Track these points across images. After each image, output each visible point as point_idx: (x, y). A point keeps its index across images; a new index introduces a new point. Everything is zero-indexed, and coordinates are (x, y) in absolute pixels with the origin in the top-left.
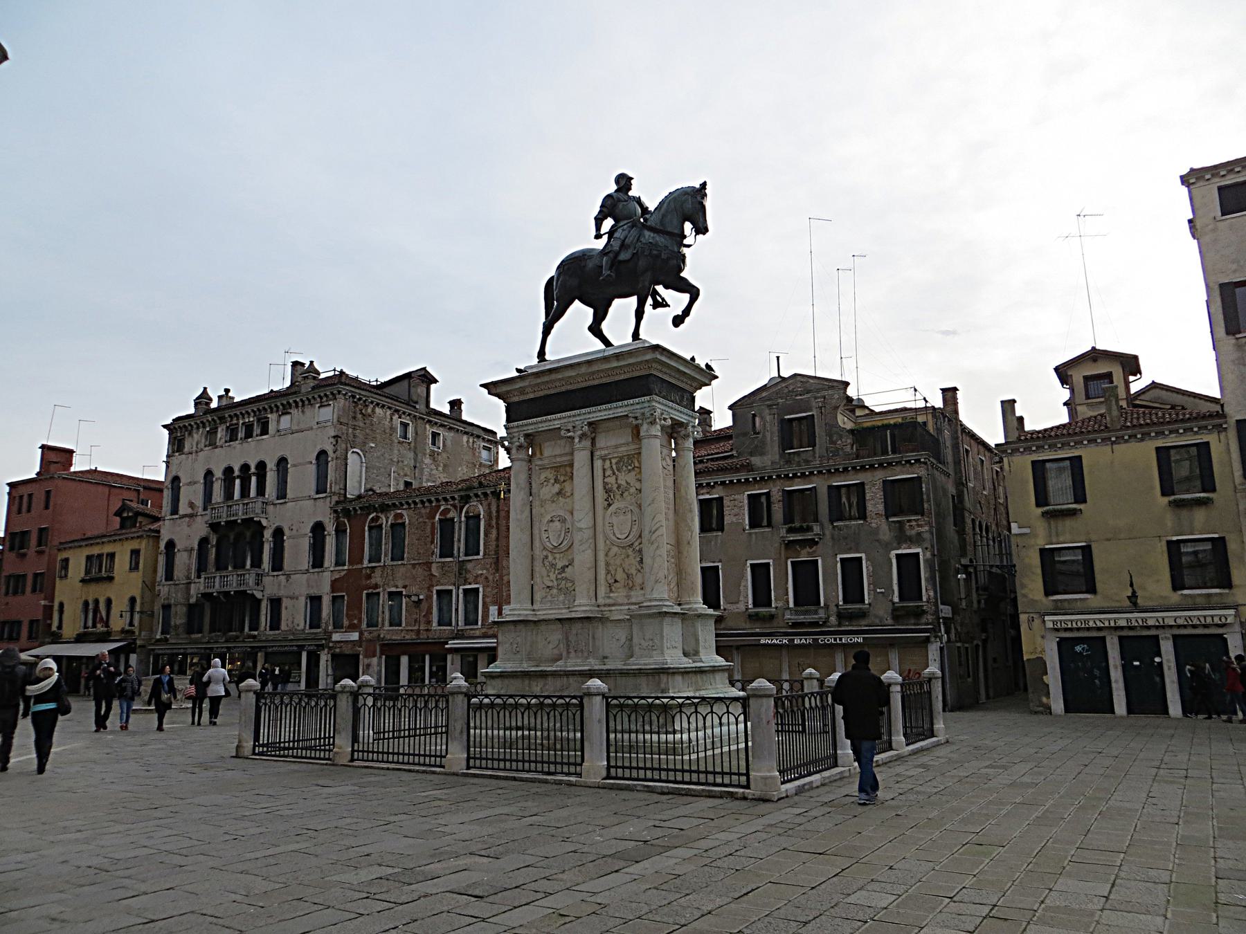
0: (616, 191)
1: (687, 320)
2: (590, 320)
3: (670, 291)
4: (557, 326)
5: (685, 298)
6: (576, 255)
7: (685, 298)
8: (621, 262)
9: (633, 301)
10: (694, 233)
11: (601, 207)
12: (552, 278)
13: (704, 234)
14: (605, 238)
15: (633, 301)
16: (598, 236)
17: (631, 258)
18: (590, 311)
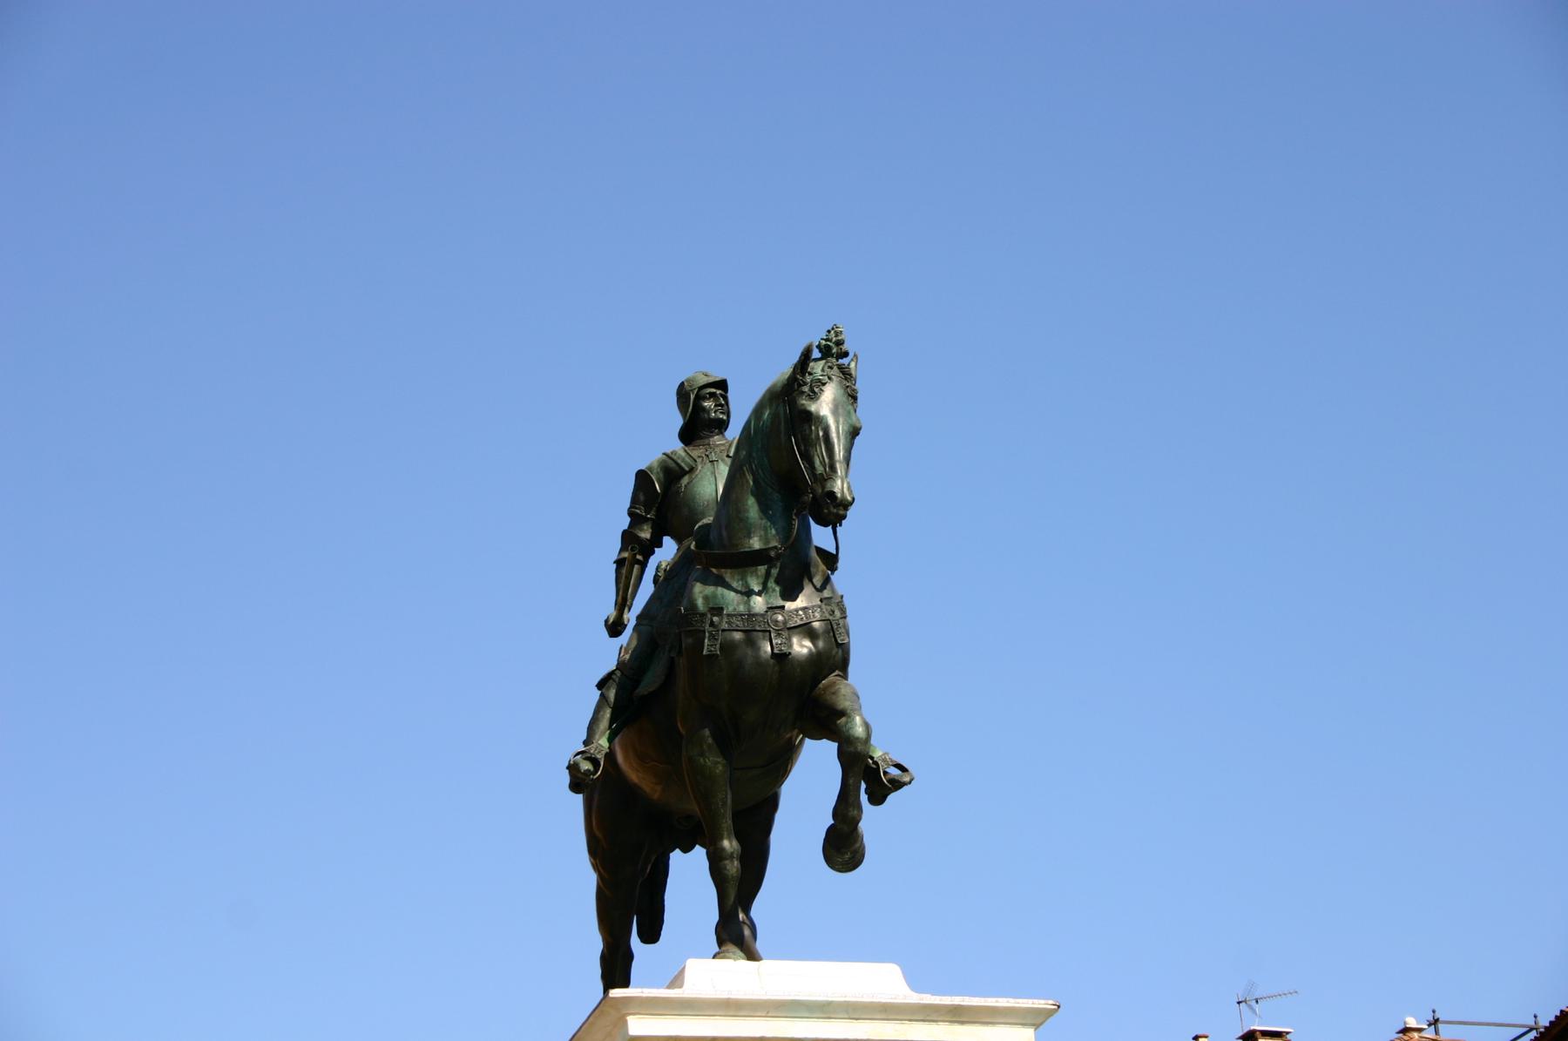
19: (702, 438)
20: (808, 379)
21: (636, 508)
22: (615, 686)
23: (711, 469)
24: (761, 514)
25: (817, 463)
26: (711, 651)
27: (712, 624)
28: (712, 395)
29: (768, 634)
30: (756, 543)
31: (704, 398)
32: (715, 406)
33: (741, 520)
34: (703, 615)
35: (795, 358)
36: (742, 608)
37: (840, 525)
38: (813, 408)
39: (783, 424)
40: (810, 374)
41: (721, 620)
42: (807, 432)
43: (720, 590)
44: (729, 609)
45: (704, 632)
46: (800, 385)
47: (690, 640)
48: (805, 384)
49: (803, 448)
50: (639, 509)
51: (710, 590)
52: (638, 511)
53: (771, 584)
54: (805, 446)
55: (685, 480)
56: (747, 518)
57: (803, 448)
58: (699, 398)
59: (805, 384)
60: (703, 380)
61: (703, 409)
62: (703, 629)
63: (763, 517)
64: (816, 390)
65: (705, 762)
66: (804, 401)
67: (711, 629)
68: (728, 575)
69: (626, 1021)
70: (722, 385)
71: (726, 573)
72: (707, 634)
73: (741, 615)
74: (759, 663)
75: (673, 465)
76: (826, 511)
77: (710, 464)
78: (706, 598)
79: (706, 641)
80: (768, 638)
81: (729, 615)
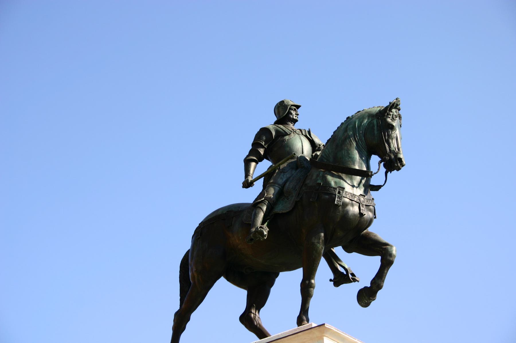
0: (276, 123)
1: (380, 293)
2: (242, 307)
3: (355, 255)
4: (194, 316)
5: (376, 261)
6: (220, 213)
7: (376, 261)
8: (277, 215)
9: (298, 274)
10: (383, 170)
11: (253, 145)
12: (188, 252)
13: (398, 169)
14: (259, 186)
15: (298, 274)
16: (247, 184)
17: (294, 209)
18: (243, 293)
19: (287, 124)
20: (391, 113)
21: (261, 142)
22: (266, 206)
23: (298, 136)
24: (360, 158)
25: (392, 146)
26: (338, 203)
27: (339, 193)
28: (295, 110)
29: (358, 204)
30: (357, 167)
31: (292, 110)
32: (296, 114)
33: (350, 157)
34: (335, 189)
35: (385, 104)
36: (351, 192)
37: (391, 173)
38: (394, 124)
39: (376, 127)
40: (392, 112)
41: (343, 192)
42: (390, 133)
43: (342, 181)
44: (346, 190)
45: (335, 195)
46: (388, 114)
47: (327, 197)
48: (390, 115)
49: (387, 138)
50: (262, 143)
51: (337, 180)
52: (261, 143)
53: (361, 185)
54: (388, 138)
55: (287, 138)
56: (354, 157)
57: (387, 138)
58: (290, 109)
59: (390, 115)
60: (292, 103)
61: (291, 114)
62: (335, 194)
63: (360, 159)
64: (395, 119)
65: (319, 246)
66: (389, 120)
67: (338, 195)
68: (344, 176)
69: (323, 338)
70: (298, 107)
71: (343, 175)
72: (337, 196)
73: (351, 193)
74: (355, 215)
75: (279, 129)
76: (396, 165)
77: (297, 135)
78: (335, 183)
79: (336, 199)
80: (358, 206)
81: (346, 192)
